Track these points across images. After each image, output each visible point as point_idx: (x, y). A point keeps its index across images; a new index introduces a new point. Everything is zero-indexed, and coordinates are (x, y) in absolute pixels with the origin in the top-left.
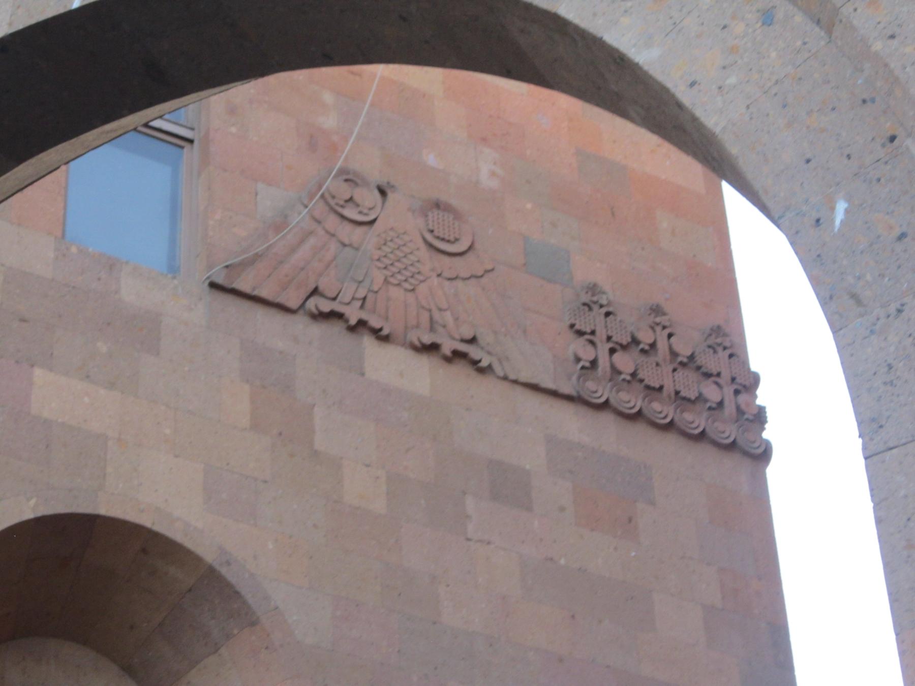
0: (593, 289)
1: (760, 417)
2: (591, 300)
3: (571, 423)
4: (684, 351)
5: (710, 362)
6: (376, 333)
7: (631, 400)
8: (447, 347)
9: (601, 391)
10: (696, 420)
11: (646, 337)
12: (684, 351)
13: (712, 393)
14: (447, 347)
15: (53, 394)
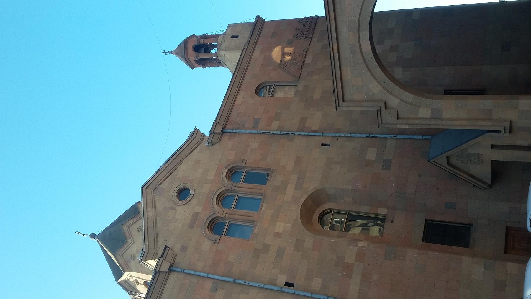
0: (294, 36)
1: (311, 17)
2: (296, 37)
3: (315, 39)
4: (302, 26)
5: (304, 23)
6: (304, 61)
7: (311, 32)
8: (305, 53)
9: (310, 36)
10: (313, 25)
11: (301, 30)
12: (302, 26)
13: (309, 22)
14: (305, 53)
15: (317, 95)
